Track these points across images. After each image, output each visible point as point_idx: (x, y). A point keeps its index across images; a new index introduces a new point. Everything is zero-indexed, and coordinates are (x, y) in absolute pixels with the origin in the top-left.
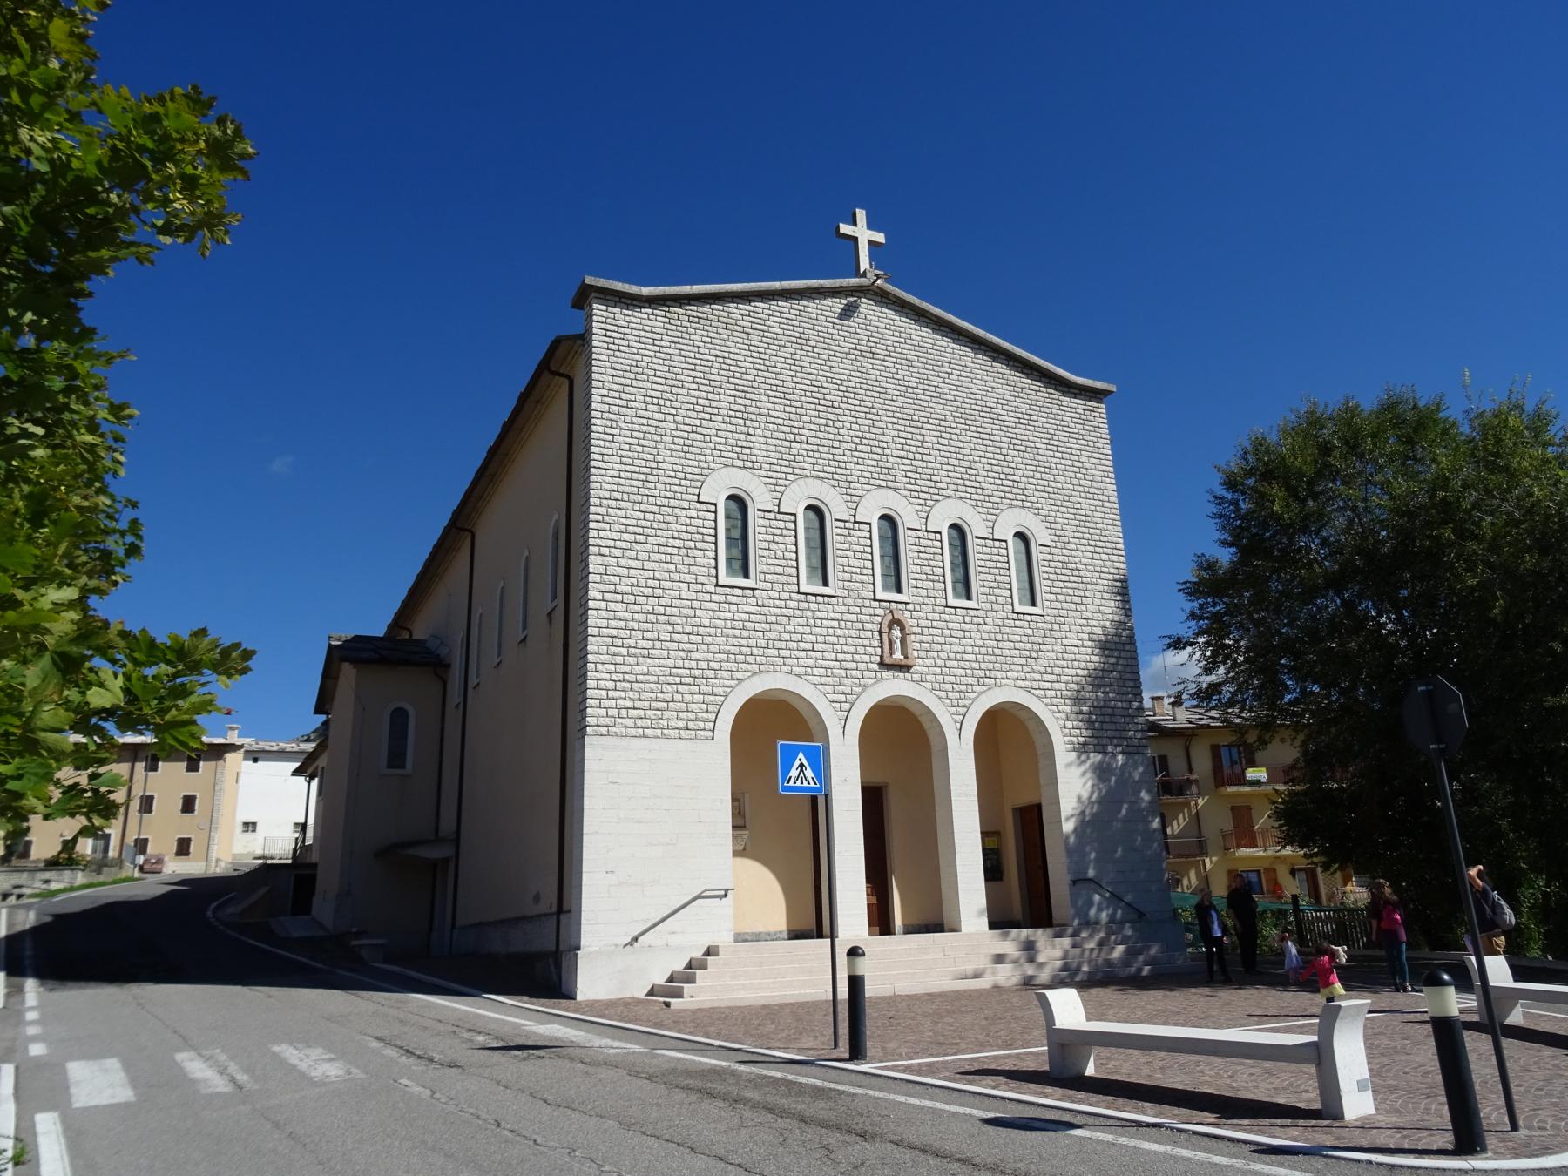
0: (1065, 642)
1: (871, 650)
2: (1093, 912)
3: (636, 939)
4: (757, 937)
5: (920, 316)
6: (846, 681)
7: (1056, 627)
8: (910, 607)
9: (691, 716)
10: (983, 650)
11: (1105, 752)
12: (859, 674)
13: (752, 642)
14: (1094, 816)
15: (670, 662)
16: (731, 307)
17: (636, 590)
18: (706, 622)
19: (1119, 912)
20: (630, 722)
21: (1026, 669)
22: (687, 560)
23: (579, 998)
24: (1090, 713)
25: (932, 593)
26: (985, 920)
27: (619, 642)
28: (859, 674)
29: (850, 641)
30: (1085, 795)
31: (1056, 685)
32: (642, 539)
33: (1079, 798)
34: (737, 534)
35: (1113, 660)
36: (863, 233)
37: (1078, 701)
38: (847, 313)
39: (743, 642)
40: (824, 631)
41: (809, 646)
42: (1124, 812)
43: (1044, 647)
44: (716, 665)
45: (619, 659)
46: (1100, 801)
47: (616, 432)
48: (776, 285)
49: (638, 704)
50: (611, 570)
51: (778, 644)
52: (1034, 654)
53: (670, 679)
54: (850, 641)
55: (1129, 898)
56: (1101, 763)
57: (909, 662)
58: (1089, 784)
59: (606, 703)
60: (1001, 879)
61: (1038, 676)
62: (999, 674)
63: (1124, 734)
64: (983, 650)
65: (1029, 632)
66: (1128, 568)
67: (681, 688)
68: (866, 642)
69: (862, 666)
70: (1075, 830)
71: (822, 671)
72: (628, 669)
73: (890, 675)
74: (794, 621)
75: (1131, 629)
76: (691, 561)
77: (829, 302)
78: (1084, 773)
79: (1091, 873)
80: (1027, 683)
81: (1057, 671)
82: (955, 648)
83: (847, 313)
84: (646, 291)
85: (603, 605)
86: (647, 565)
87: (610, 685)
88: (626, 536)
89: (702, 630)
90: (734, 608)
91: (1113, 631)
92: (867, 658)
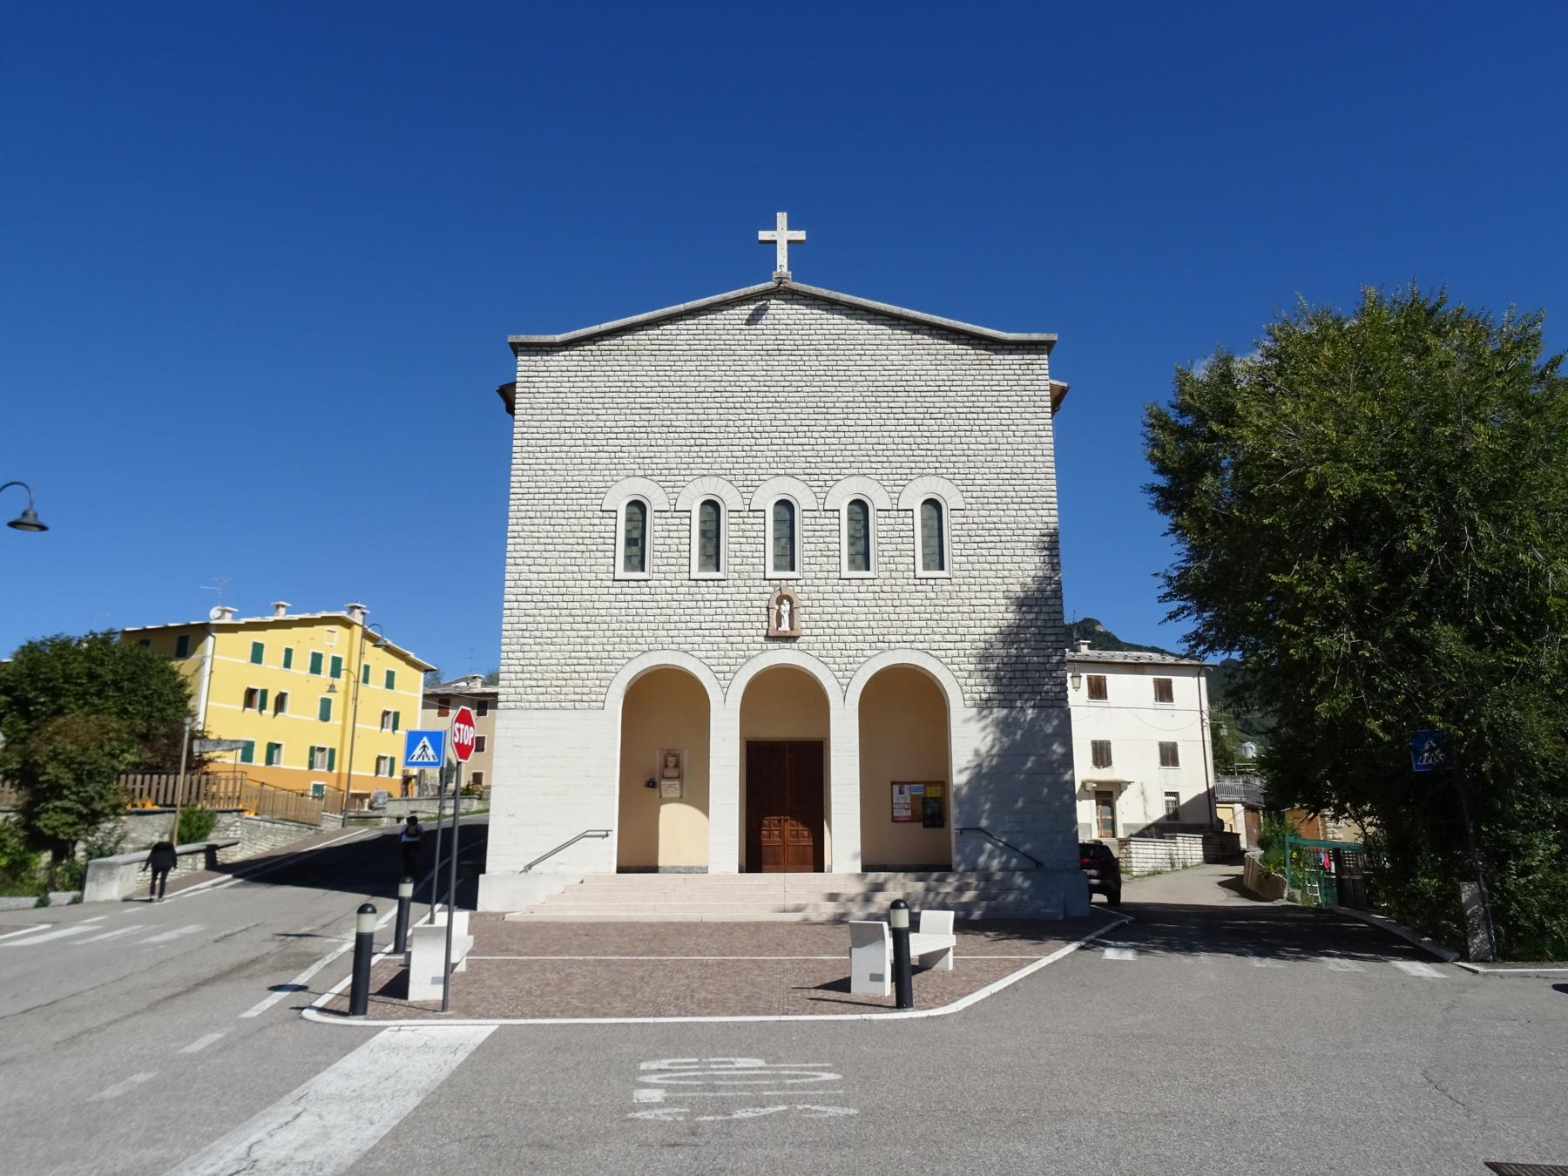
0: (974, 602)
1: (758, 625)
2: (982, 859)
3: (530, 866)
4: (689, 870)
5: (831, 305)
6: (731, 654)
7: (964, 588)
8: (801, 582)
9: (586, 690)
10: (878, 617)
11: (1012, 708)
12: (744, 647)
13: (644, 626)
14: (992, 768)
15: (570, 648)
16: (641, 335)
17: (544, 591)
18: (603, 612)
19: (1014, 861)
21: (925, 631)
22: (589, 562)
23: (480, 908)
24: (998, 669)
25: (826, 567)
26: (858, 863)
27: (527, 634)
28: (744, 647)
29: (737, 618)
30: (983, 749)
31: (959, 645)
32: (551, 547)
33: (977, 753)
35: (1031, 616)
36: (782, 234)
37: (984, 657)
38: (753, 319)
39: (636, 626)
41: (696, 626)
42: (1029, 764)
43: (947, 609)
44: (609, 648)
45: (527, 648)
48: (681, 307)
50: (523, 576)
51: (667, 626)
52: (935, 617)
53: (569, 661)
54: (737, 618)
55: (1027, 847)
56: (1006, 717)
57: (794, 633)
58: (990, 738)
59: (514, 683)
60: (942, 825)
61: (937, 638)
62: (893, 638)
63: (1037, 689)
64: (878, 617)
65: (933, 595)
66: (1060, 522)
67: (578, 668)
68: (753, 618)
69: (748, 639)
70: (969, 782)
71: (709, 647)
72: (533, 655)
73: (776, 645)
74: (684, 604)
75: (1059, 583)
76: (593, 562)
77: (737, 311)
78: (985, 728)
79: (984, 823)
80: (926, 645)
81: (961, 631)
82: (846, 617)
83: (753, 319)
84: (558, 338)
85: (515, 605)
86: (554, 569)
87: (519, 669)
88: (537, 547)
89: (599, 619)
90: (629, 598)
91: (1034, 587)
92: (753, 632)
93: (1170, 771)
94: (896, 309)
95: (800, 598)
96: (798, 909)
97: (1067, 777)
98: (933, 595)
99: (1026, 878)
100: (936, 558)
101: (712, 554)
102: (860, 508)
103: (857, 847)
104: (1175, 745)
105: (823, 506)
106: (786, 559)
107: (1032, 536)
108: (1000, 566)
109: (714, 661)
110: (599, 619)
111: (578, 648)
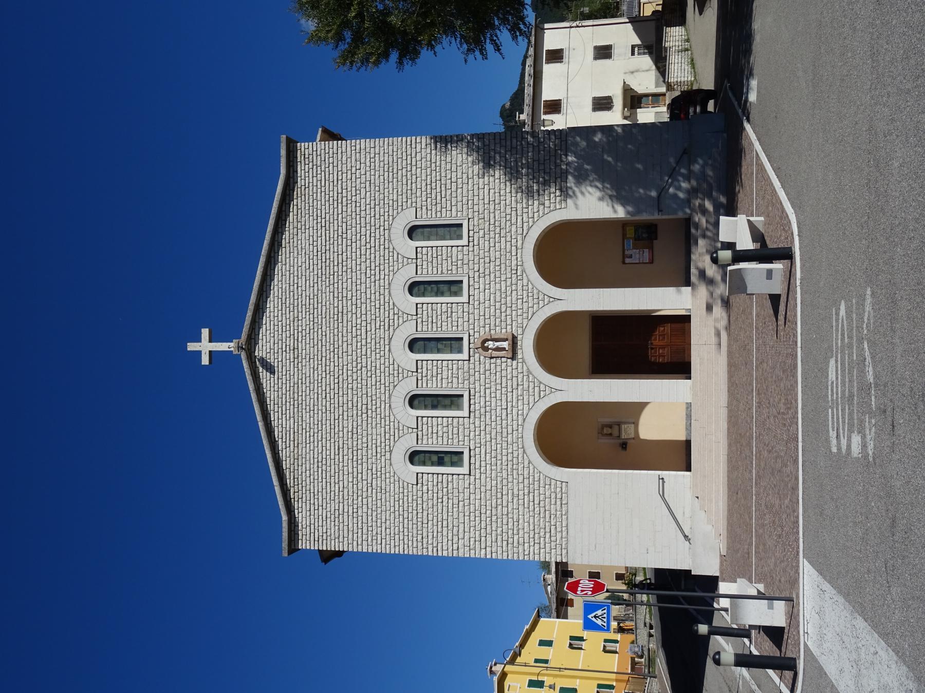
0: (486, 201)
1: (504, 365)
2: (681, 195)
3: (686, 537)
4: (689, 417)
5: (260, 309)
6: (526, 386)
7: (476, 208)
8: (472, 332)
9: (553, 496)
10: (498, 274)
11: (567, 172)
12: (520, 376)
14: (612, 188)
15: (521, 508)
16: (283, 454)
17: (478, 528)
18: (494, 483)
19: (683, 171)
20: (559, 536)
21: (508, 239)
22: (456, 494)
23: (717, 574)
24: (538, 183)
26: (684, 289)
27: (510, 540)
28: (520, 376)
29: (498, 381)
31: (519, 213)
34: (435, 458)
35: (498, 157)
37: (529, 193)
38: (270, 369)
39: (505, 458)
40: (494, 400)
41: (504, 412)
42: (610, 159)
43: (492, 221)
45: (521, 540)
46: (603, 181)
47: (379, 536)
49: (548, 530)
50: (467, 543)
51: (505, 434)
52: (498, 230)
53: (531, 508)
54: (498, 381)
55: (672, 160)
56: (575, 177)
57: (510, 338)
58: (590, 189)
59: (548, 550)
60: (656, 226)
62: (514, 263)
63: (553, 153)
64: (498, 274)
65: (481, 232)
66: (426, 135)
67: (536, 502)
68: (499, 369)
70: (623, 205)
71: (520, 403)
72: (526, 535)
73: (519, 352)
74: (488, 421)
75: (472, 136)
76: (456, 491)
78: (582, 193)
79: (654, 194)
80: (519, 237)
81: (508, 211)
82: (498, 299)
83: (270, 369)
84: (285, 518)
85: (488, 549)
86: (461, 520)
87: (537, 546)
88: (445, 533)
89: (499, 486)
90: (483, 464)
91: (475, 154)
92: (509, 369)
93: (615, 52)
94: (262, 260)
95: (483, 333)
96: (718, 334)
97: (619, 130)
98: (481, 232)
99: (696, 162)
100: (453, 230)
101: (450, 401)
102: (415, 288)
103: (672, 290)
104: (596, 48)
105: (413, 315)
106: (452, 344)
107: (436, 156)
108: (460, 181)
109: (531, 399)
110: (499, 486)
111: (521, 502)
